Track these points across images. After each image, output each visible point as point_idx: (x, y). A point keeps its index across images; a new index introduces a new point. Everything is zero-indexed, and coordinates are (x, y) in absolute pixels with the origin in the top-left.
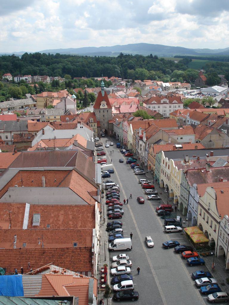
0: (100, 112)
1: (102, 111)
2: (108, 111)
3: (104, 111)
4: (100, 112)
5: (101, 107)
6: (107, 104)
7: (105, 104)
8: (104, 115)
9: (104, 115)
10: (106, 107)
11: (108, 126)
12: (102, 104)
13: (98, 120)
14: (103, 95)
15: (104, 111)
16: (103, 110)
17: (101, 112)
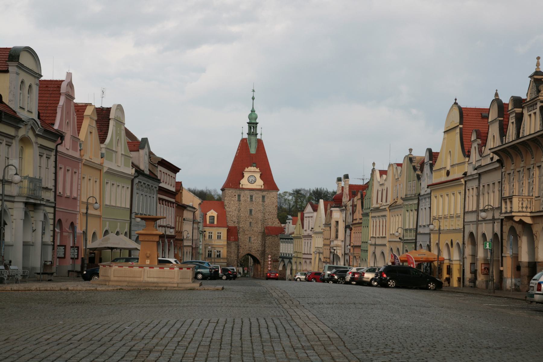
0: (239, 200)
1: (245, 196)
2: (263, 197)
3: (251, 197)
4: (239, 200)
5: (244, 183)
6: (261, 177)
7: (258, 176)
8: (251, 211)
9: (251, 211)
10: (259, 183)
11: (264, 245)
12: (246, 175)
13: (231, 224)
14: (253, 151)
15: (251, 197)
16: (247, 192)
17: (242, 198)
